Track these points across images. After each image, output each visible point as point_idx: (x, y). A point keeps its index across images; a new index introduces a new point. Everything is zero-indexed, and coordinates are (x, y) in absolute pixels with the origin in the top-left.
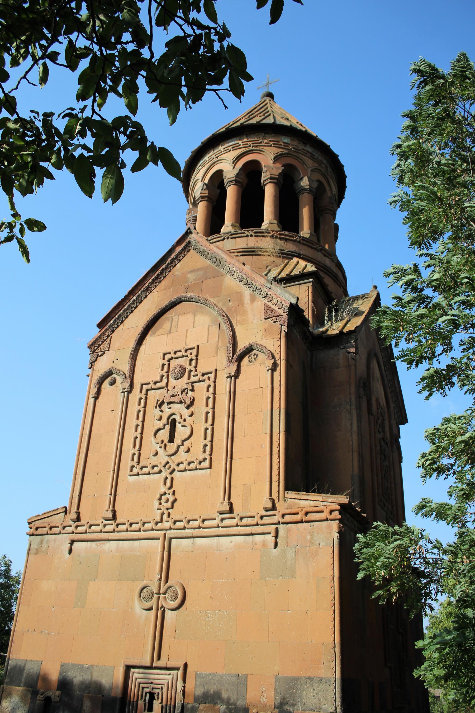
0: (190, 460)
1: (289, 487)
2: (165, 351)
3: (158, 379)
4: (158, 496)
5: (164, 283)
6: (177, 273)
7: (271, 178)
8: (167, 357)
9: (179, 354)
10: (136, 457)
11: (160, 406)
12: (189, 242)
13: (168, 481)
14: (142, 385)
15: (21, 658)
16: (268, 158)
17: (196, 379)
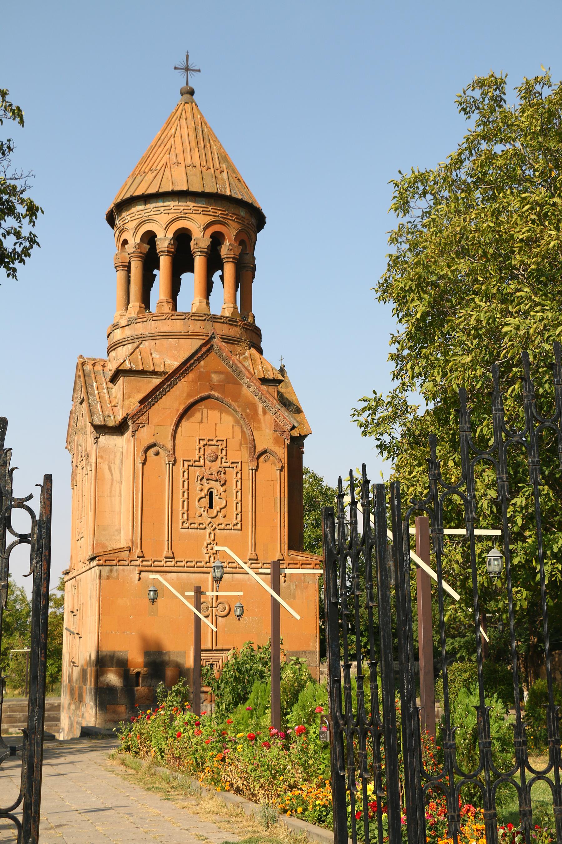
0: (225, 523)
1: (290, 548)
2: (201, 438)
3: (197, 459)
4: (206, 545)
5: (191, 376)
6: (202, 370)
7: (234, 258)
8: (202, 442)
9: (211, 443)
10: (185, 516)
11: (201, 480)
12: (212, 345)
13: (212, 535)
14: (184, 461)
15: (109, 650)
16: (230, 233)
17: (227, 465)
